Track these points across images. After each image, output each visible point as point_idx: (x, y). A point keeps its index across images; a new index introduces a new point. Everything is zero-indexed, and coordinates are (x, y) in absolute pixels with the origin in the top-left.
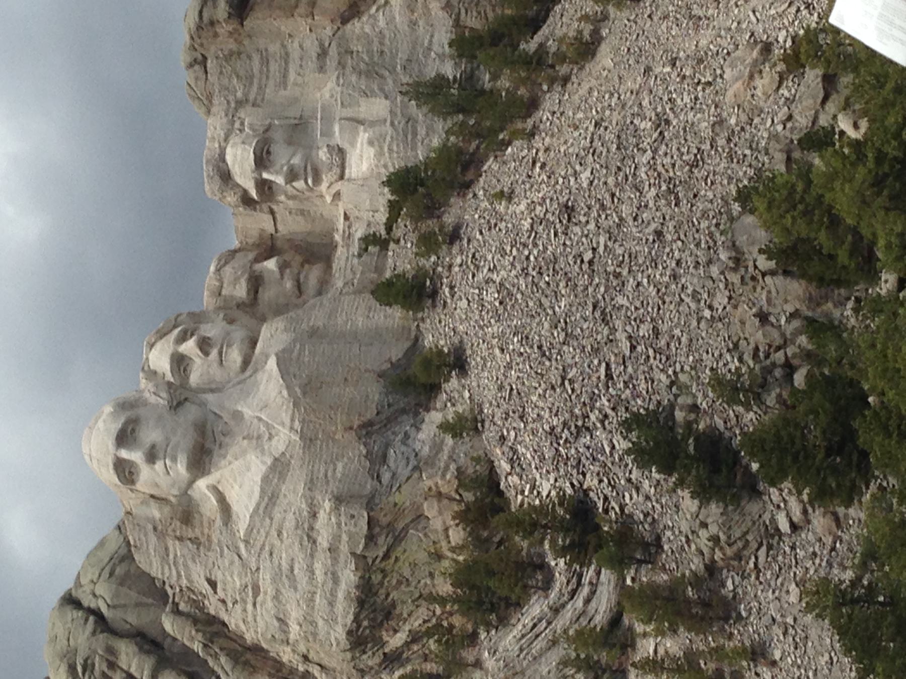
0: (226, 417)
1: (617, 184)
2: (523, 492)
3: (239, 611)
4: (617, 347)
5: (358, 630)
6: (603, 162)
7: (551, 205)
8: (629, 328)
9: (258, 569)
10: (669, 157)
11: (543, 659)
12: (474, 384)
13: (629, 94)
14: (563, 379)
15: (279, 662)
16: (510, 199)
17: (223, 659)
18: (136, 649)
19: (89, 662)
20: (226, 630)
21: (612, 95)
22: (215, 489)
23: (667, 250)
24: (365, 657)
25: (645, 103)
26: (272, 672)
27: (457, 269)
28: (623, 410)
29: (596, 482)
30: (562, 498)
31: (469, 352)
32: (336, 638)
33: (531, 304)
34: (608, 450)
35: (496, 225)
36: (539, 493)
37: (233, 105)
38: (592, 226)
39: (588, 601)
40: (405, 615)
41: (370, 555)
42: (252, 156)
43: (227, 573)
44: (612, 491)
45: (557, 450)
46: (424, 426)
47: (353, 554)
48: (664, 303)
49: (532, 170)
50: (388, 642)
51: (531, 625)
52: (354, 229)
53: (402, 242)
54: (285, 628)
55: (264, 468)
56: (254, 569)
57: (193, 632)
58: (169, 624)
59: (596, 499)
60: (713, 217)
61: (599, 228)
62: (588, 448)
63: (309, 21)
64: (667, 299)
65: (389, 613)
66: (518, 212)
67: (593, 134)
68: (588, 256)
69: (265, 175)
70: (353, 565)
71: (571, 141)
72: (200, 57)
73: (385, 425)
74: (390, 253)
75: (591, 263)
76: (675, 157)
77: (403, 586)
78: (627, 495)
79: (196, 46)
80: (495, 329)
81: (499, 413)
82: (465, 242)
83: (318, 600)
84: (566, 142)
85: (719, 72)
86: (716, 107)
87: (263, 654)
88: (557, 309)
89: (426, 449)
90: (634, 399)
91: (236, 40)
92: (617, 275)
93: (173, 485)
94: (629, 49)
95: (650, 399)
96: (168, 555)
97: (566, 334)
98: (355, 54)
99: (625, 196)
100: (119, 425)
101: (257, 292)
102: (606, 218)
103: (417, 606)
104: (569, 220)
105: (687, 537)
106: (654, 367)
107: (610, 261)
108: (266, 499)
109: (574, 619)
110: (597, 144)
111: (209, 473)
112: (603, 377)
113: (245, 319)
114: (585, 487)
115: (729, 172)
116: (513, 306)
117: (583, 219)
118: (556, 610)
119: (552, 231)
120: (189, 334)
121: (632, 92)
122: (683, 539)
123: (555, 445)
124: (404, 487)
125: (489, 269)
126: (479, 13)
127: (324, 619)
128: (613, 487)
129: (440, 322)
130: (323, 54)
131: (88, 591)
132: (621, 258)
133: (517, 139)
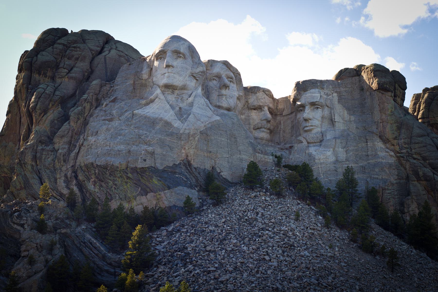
0: (191, 99)
2: (158, 237)
8: (232, 279)
9: (120, 120)
13: (346, 270)
14: (210, 251)
19: (78, 49)
21: (345, 263)
25: (342, 279)
30: (153, 255)
31: (224, 207)
33: (245, 234)
34: (175, 274)
36: (158, 244)
38: (282, 258)
39: (107, 271)
40: (101, 189)
45: (176, 251)
50: (90, 182)
54: (94, 134)
56: (120, 118)
57: (91, 94)
58: (95, 83)
65: (102, 181)
68: (267, 258)
69: (307, 108)
73: (190, 172)
75: (264, 259)
82: (276, 201)
84: (324, 243)
87: (83, 126)
88: (243, 245)
92: (257, 272)
96: (126, 79)
97: (230, 251)
101: (254, 109)
102: (285, 265)
103: (106, 194)
104: (284, 247)
107: (264, 268)
111: (164, 94)
112: (209, 269)
116: (244, 225)
117: (286, 254)
120: (231, 80)
121: (347, 272)
126: (389, 199)
127: (98, 152)
128: (158, 279)
132: (266, 273)
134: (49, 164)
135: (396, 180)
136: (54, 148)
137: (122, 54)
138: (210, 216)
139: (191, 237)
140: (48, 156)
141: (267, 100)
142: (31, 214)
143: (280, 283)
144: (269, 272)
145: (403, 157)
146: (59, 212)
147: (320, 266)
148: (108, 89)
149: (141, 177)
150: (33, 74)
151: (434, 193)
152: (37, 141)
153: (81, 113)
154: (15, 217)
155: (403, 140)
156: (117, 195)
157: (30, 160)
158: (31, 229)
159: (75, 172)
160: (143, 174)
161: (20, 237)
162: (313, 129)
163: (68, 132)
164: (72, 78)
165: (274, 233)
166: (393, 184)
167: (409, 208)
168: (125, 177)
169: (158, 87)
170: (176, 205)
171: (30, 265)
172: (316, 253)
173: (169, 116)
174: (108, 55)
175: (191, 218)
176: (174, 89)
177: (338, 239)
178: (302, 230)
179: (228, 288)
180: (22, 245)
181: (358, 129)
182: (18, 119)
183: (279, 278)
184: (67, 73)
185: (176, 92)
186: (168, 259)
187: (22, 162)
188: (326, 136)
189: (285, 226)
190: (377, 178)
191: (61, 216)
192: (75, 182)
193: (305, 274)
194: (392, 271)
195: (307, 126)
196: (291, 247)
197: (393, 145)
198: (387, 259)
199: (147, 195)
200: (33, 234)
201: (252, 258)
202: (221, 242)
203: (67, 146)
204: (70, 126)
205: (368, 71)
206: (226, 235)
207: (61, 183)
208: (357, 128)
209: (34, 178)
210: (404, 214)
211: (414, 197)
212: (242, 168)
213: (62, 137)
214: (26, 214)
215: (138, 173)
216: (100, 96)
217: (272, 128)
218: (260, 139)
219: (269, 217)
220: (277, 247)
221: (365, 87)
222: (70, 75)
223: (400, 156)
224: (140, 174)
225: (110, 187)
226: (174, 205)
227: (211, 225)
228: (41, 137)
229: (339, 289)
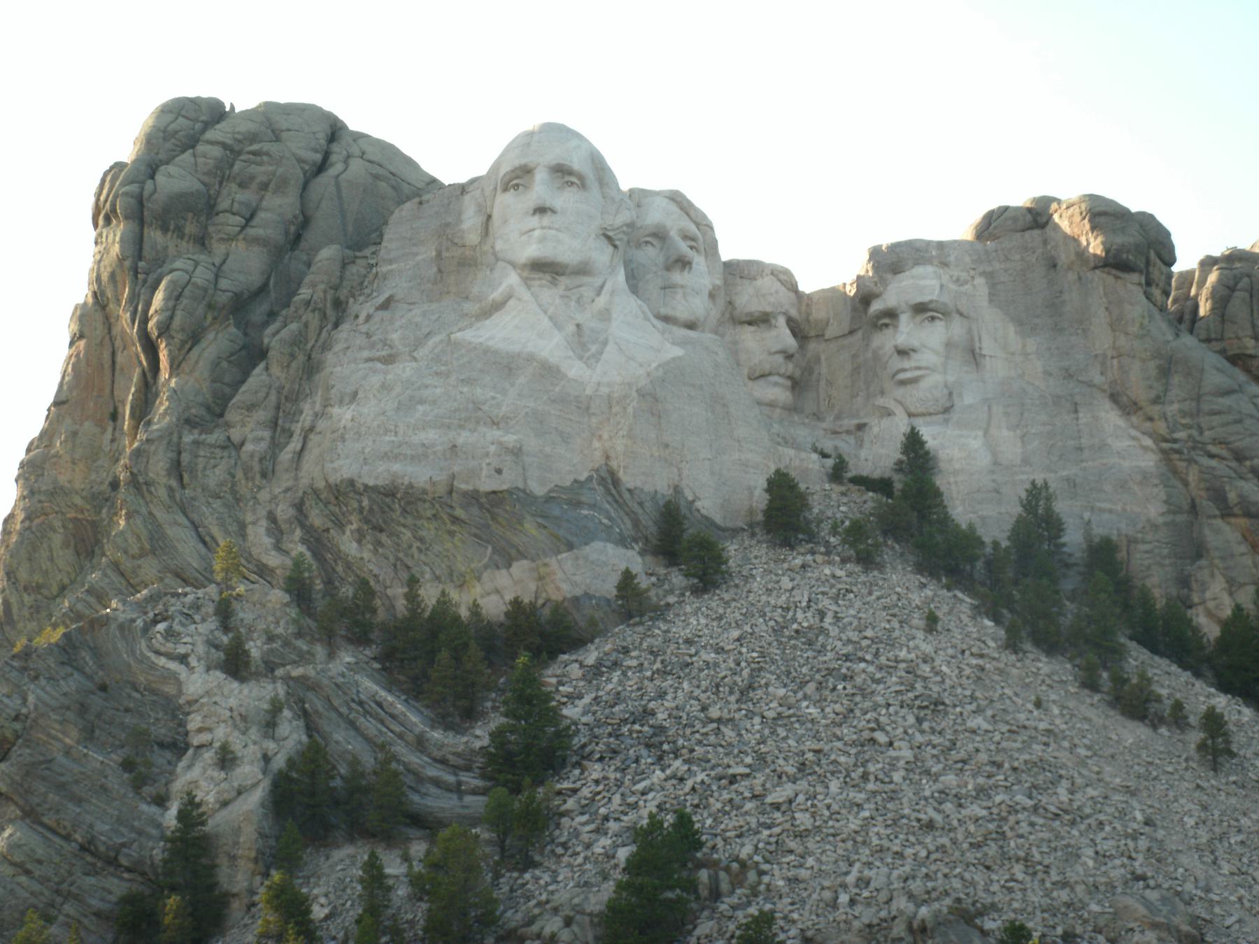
0: (602, 301)
2: (561, 683)
3: (358, 342)
4: (774, 786)
5: (355, 492)
7: (935, 683)
8: (801, 798)
9: (415, 359)
10: (1029, 829)
11: (352, 733)
12: (688, 609)
13: (1096, 769)
14: (719, 721)
17: (294, 326)
18: (289, 216)
19: (265, 158)
21: (1088, 748)
22: (508, 297)
23: (912, 839)
25: (1091, 792)
26: (285, 392)
27: (827, 571)
28: (696, 802)
29: (595, 776)
31: (727, 596)
33: (804, 670)
34: (640, 786)
35: (894, 615)
36: (564, 704)
37: (989, 269)
38: (919, 738)
39: (437, 783)
40: (381, 550)
42: (926, 299)
43: (404, 321)
45: (625, 721)
47: (453, 477)
48: (843, 841)
49: (972, 654)
50: (344, 533)
51: (395, 712)
53: (845, 500)
54: (347, 400)
55: (545, 354)
56: (415, 354)
57: (322, 286)
58: (328, 254)
59: (572, 779)
60: (967, 894)
61: (919, 748)
63: (1109, 353)
64: (850, 844)
65: (381, 531)
66: (917, 641)
68: (881, 737)
69: (904, 318)
70: (439, 479)
71: (1020, 701)
73: (616, 501)
74: (827, 486)
76: (1032, 837)
77: (418, 544)
78: (585, 818)
80: (762, 627)
81: (657, 642)
83: (387, 438)
84: (1016, 695)
85: (1152, 883)
86: (1106, 884)
87: (305, 377)
88: (805, 704)
89: (594, 557)
90: (710, 815)
91: (1072, 263)
94: (1150, 763)
95: (716, 835)
96: (415, 245)
97: (774, 719)
98: (1074, 416)
99: (967, 776)
100: (576, 166)
101: (750, 323)
102: (934, 756)
103: (395, 566)
104: (920, 708)
105: (547, 902)
106: (758, 836)
107: (880, 766)
111: (529, 287)
112: (731, 771)
113: (715, 314)
115: (1030, 909)
116: (794, 647)
117: (926, 725)
119: (903, 688)
120: (693, 244)
121: (1098, 773)
122: (544, 897)
123: (631, 720)
125: (836, 612)
126: (1149, 568)
127: (364, 448)
129: (756, 557)
132: (887, 780)
133: (1007, 632)
134: (221, 485)
135: (1163, 514)
136: (229, 438)
138: (693, 621)
139: (657, 682)
140: (212, 461)
141: (785, 297)
142: (199, 626)
143: (935, 809)
145: (1178, 452)
146: (271, 618)
147: (1027, 757)
148: (363, 271)
149: (492, 515)
150: (146, 230)
152: (178, 420)
153: (298, 341)
154: (158, 636)
155: (1175, 406)
156: (428, 569)
157: (163, 473)
158: (208, 669)
159: (299, 506)
160: (496, 510)
161: (180, 693)
163: (268, 394)
164: (256, 240)
165: (881, 669)
166: (1155, 527)
167: (1203, 591)
168: (445, 517)
169: (510, 267)
170: (591, 592)
171: (223, 768)
172: (1007, 723)
173: (551, 346)
174: (343, 176)
175: (640, 629)
176: (557, 274)
177: (1048, 681)
178: (953, 657)
179: (798, 822)
180: (188, 714)
181: (1050, 374)
182: (106, 356)
183: (927, 793)
184: (243, 228)
185: (564, 281)
186: (608, 744)
187: (141, 479)
188: (960, 395)
189: (905, 649)
190: (1111, 511)
191: (280, 630)
192: (298, 533)
193: (991, 781)
194: (1215, 770)
195: (904, 370)
196: (936, 704)
197: (1151, 419)
198: (1195, 736)
199: (510, 565)
200: (215, 683)
201: (839, 739)
202: (745, 693)
203: (267, 434)
204: (270, 375)
205: (1072, 216)
206: (751, 676)
207: (259, 537)
208: (1047, 373)
209: (176, 523)
210: (1190, 607)
213: (251, 407)
214: (183, 625)
215: (481, 506)
216: (343, 294)
217: (797, 374)
218: (767, 405)
219: (855, 623)
220: (898, 708)
221: (1064, 259)
222: (251, 231)
224: (488, 510)
225: (405, 546)
226: (586, 594)
227: (704, 647)
228: (188, 408)
229: (1091, 821)
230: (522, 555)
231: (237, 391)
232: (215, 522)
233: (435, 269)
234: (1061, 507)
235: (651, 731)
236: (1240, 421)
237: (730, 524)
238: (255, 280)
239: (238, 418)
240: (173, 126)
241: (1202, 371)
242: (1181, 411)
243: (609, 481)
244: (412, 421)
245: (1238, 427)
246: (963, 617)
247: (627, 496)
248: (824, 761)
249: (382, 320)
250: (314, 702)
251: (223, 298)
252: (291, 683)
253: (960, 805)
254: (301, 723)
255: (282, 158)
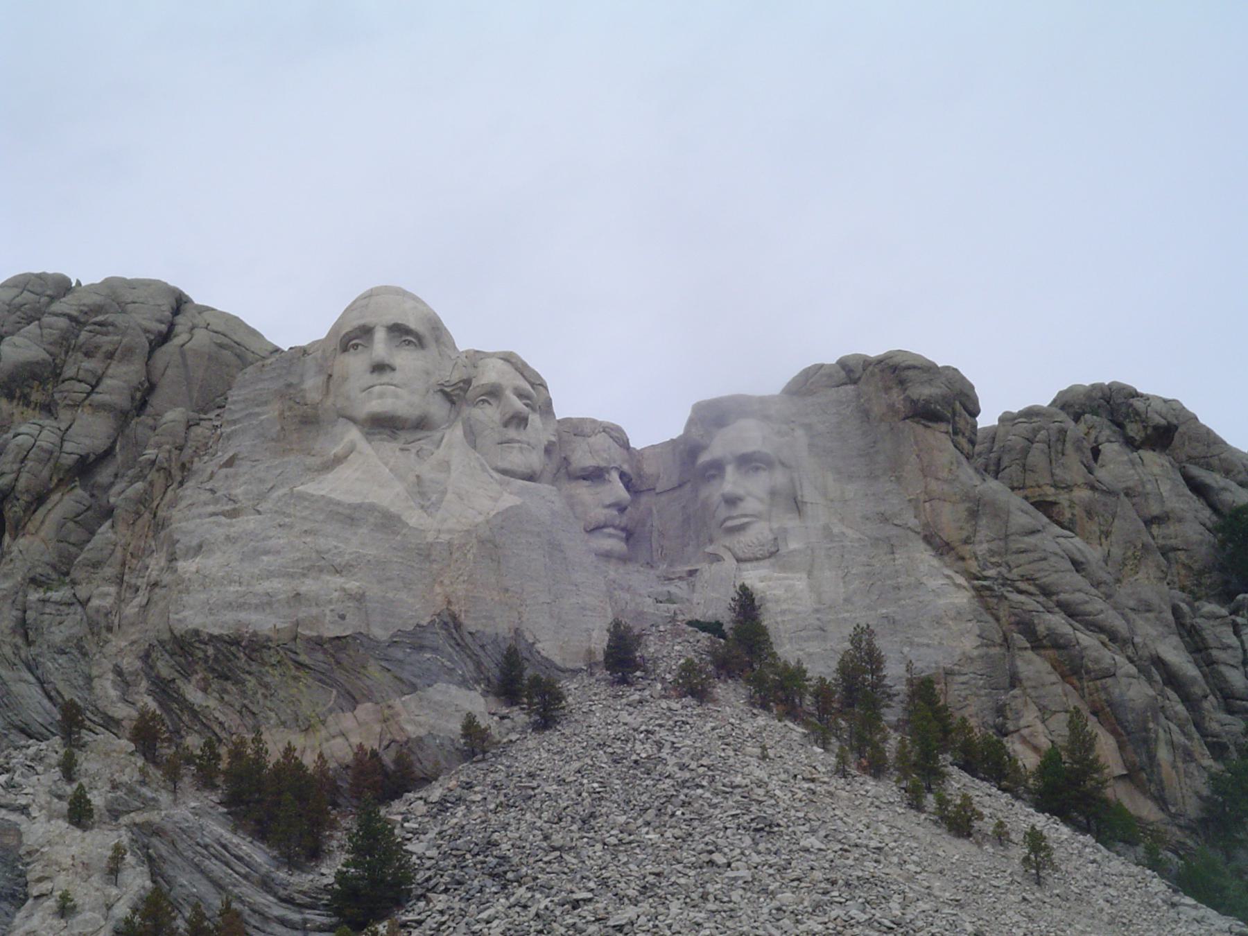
0: (440, 453)
1: (814, 883)
2: (406, 820)
4: (617, 909)
5: (201, 642)
6: (837, 862)
8: (643, 919)
9: (259, 513)
11: (198, 876)
12: (531, 744)
13: (926, 884)
15: (143, 553)
16: (764, 757)
19: (111, 328)
20: (175, 485)
21: (918, 864)
22: (352, 449)
24: (167, 656)
26: (131, 548)
27: (664, 705)
28: (540, 927)
29: (440, 906)
32: (185, 618)
33: (644, 798)
34: (484, 915)
36: (409, 840)
38: (756, 859)
39: (283, 922)
40: (226, 697)
41: (300, 646)
44: (431, 929)
46: (463, 692)
47: (297, 624)
49: (804, 779)
50: (189, 681)
51: (241, 853)
52: (679, 583)
57: (168, 447)
58: (174, 416)
62: (481, 891)
63: (922, 497)
65: (227, 678)
66: (751, 768)
67: (867, 846)
68: (718, 858)
69: (730, 470)
70: (283, 626)
72: (857, 376)
73: (458, 645)
75: (711, 863)
77: (263, 690)
79: (870, 368)
81: (500, 776)
83: (232, 589)
84: (846, 815)
87: (151, 534)
88: (645, 830)
89: (438, 697)
92: (704, 897)
93: (348, 398)
94: (978, 877)
96: (258, 405)
100: (412, 325)
103: (240, 712)
104: (756, 830)
108: (348, 511)
109: (256, 908)
110: (856, 853)
112: (575, 896)
114: (429, 895)
117: (762, 847)
118: (266, 884)
121: (928, 888)
124: (388, 675)
126: (965, 698)
129: (595, 694)
130: (884, 519)
131: (196, 322)
132: (726, 899)
135: (977, 647)
137: (226, 341)
141: (617, 453)
144: (735, 896)
147: (860, 874)
148: (208, 433)
149: (334, 660)
151: (1080, 679)
153: (143, 501)
155: (985, 546)
156: (273, 714)
157: (7, 631)
159: (146, 657)
161: (20, 843)
162: (747, 523)
163: (113, 551)
167: (1018, 719)
170: (435, 732)
172: (839, 841)
177: (877, 803)
180: (28, 864)
184: (89, 394)
185: (404, 436)
188: (785, 540)
190: (928, 646)
191: (125, 778)
197: (963, 559)
198: (1019, 852)
204: (115, 533)
207: (107, 689)
210: (1006, 735)
211: (1029, 691)
212: (587, 630)
213: (96, 565)
215: (325, 652)
223: (982, 586)
224: (333, 656)
230: (368, 698)
231: (82, 549)
232: (60, 677)
233: (279, 428)
234: (882, 644)
235: (495, 861)
236: (1045, 559)
237: (570, 665)
238: (101, 444)
239: (84, 575)
240: (19, 300)
241: (1008, 513)
242: (990, 550)
243: (452, 625)
244: (257, 571)
245: (1044, 564)
246: (794, 744)
247: (469, 639)
248: (664, 884)
249: (227, 476)
250: (160, 847)
251: (68, 460)
252: (135, 829)
253: (797, 921)
254: (146, 869)
255: (127, 328)
